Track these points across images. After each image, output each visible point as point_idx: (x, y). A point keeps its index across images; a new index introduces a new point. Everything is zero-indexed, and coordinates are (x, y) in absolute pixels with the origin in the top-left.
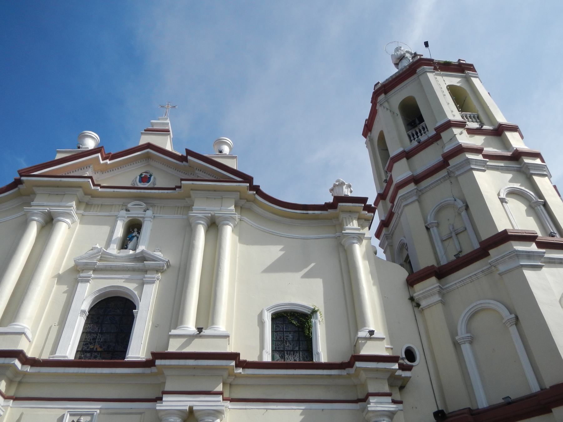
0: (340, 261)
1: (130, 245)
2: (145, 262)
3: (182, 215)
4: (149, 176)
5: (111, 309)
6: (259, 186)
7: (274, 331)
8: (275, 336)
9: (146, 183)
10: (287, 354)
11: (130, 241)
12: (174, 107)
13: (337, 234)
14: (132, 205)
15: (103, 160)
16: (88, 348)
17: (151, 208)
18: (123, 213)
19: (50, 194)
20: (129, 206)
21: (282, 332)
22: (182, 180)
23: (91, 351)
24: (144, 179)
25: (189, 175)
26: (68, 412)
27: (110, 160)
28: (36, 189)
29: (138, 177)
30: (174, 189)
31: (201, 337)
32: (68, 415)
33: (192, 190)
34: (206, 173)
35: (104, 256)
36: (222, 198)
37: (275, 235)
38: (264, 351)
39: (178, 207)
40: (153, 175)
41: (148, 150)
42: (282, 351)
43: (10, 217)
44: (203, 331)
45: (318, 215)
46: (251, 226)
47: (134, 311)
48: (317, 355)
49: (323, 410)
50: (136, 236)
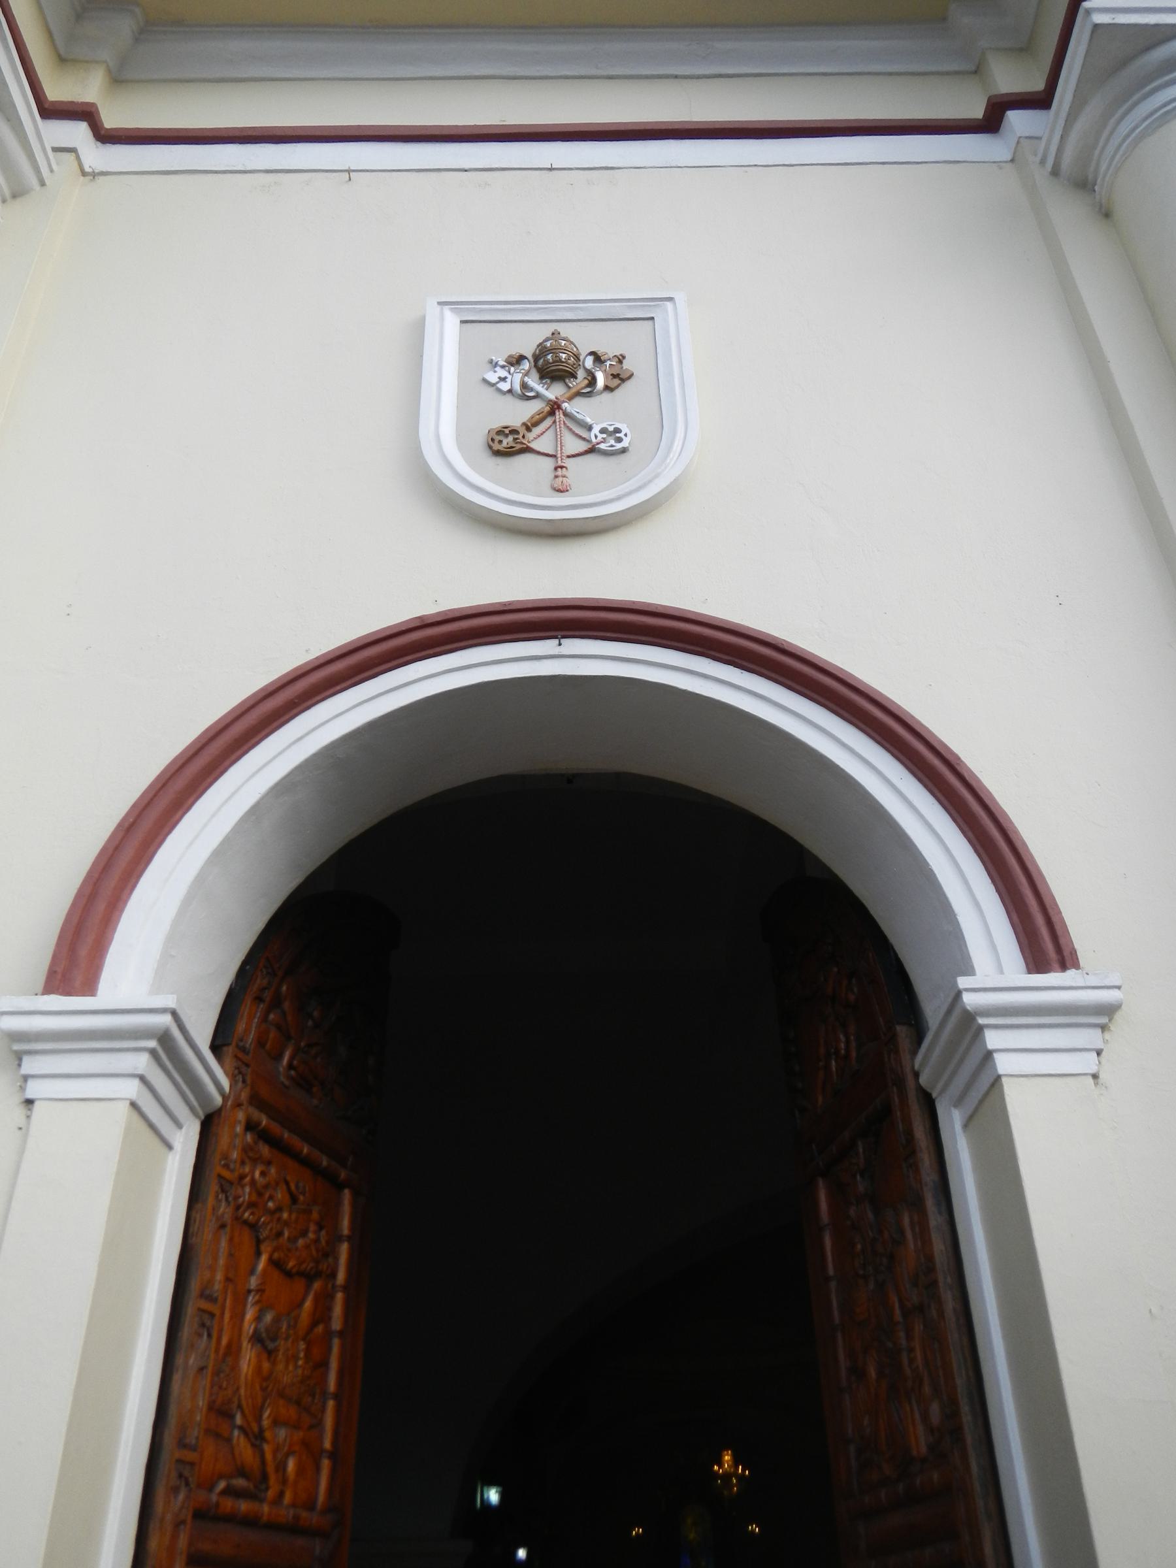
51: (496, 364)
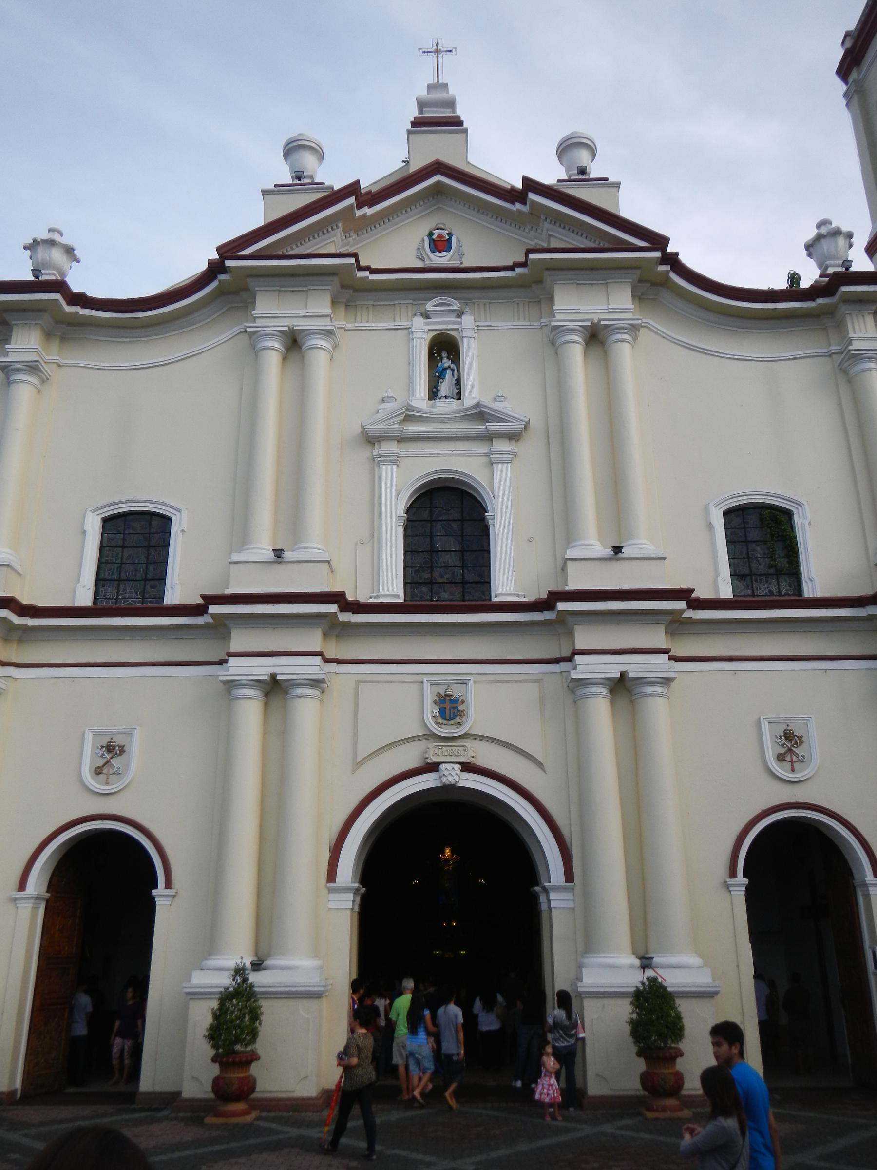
0: (840, 405)
1: (445, 387)
2: (487, 424)
3: (529, 321)
4: (447, 237)
5: (440, 509)
6: (677, 254)
7: (731, 541)
8: (732, 550)
9: (444, 254)
10: (756, 581)
11: (442, 380)
12: (451, 51)
13: (832, 348)
14: (435, 306)
15: (359, 208)
16: (421, 577)
17: (467, 310)
18: (419, 322)
19: (279, 291)
20: (429, 306)
21: (744, 544)
22: (529, 251)
23: (430, 583)
24: (440, 244)
25: (527, 230)
26: (427, 680)
27: (371, 205)
28: (251, 282)
29: (427, 240)
30: (511, 268)
31: (618, 559)
32: (429, 685)
33: (547, 269)
34: (575, 232)
35: (410, 416)
36: (606, 283)
37: (711, 355)
38: (719, 578)
39: (518, 304)
40: (453, 232)
41: (438, 178)
42: (747, 575)
43: (217, 340)
44: (623, 550)
45: (795, 309)
46: (664, 337)
47: (486, 514)
48: (810, 583)
49: (826, 671)
50: (449, 367)
51: (777, 737)
